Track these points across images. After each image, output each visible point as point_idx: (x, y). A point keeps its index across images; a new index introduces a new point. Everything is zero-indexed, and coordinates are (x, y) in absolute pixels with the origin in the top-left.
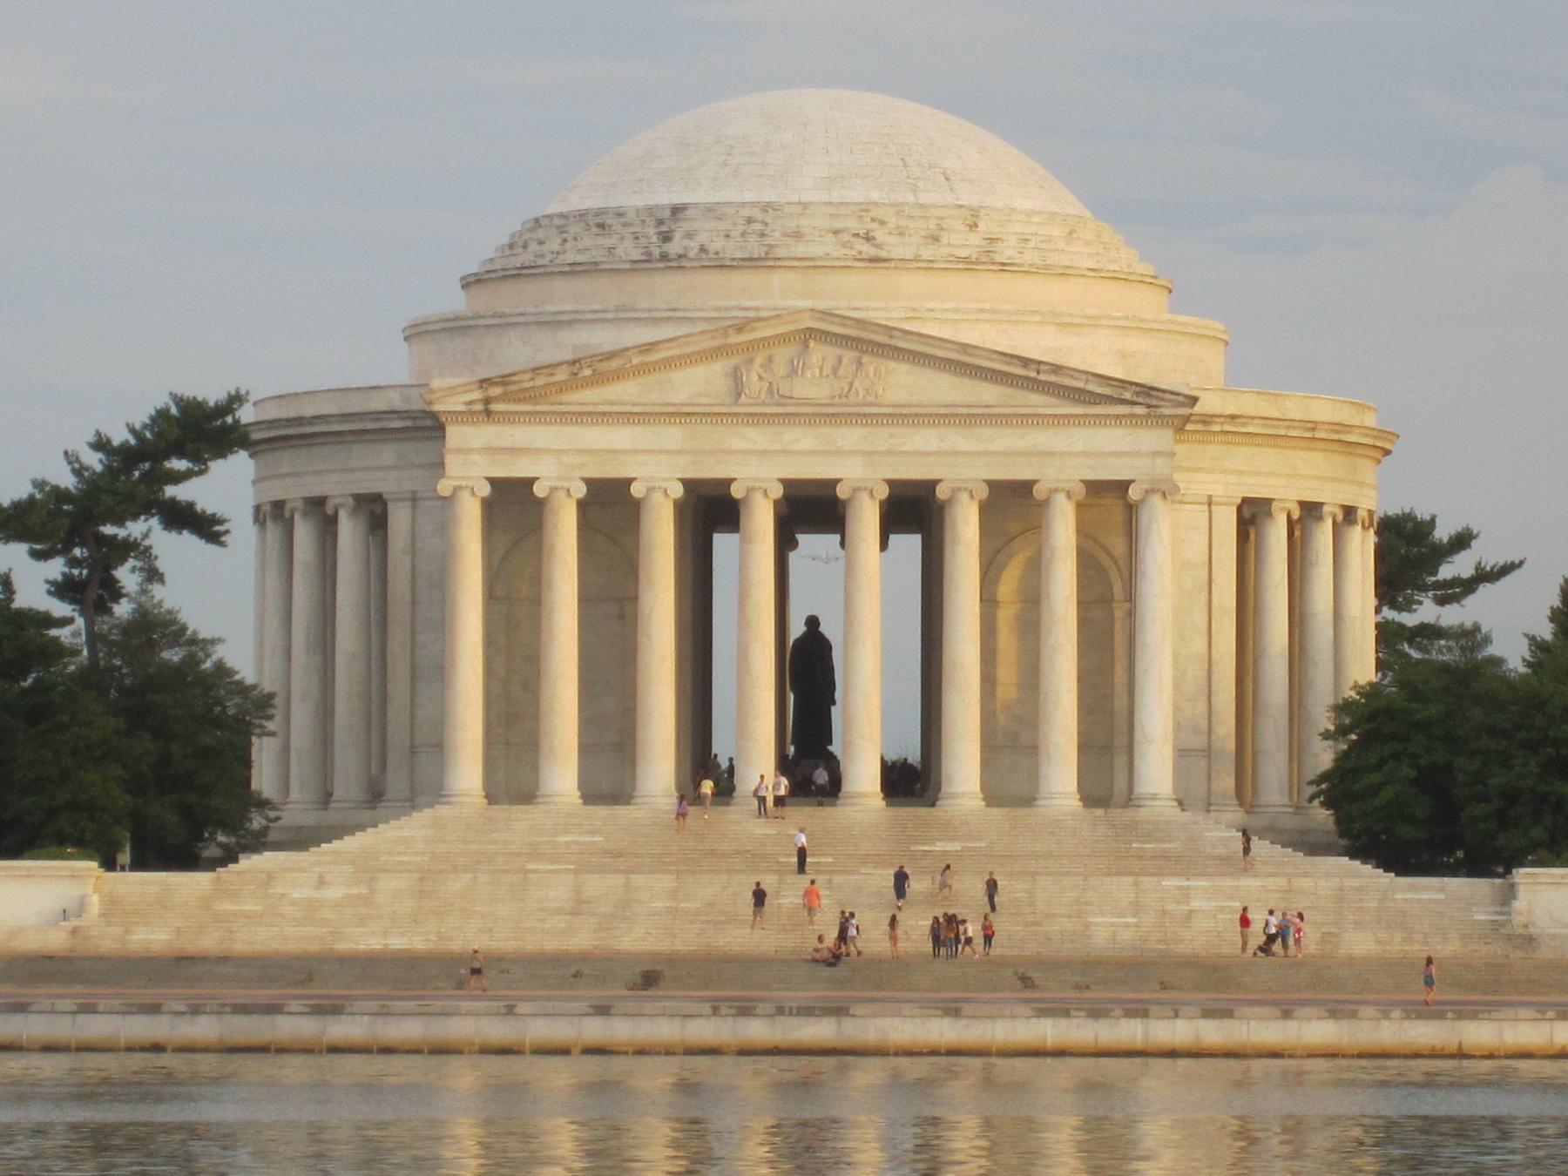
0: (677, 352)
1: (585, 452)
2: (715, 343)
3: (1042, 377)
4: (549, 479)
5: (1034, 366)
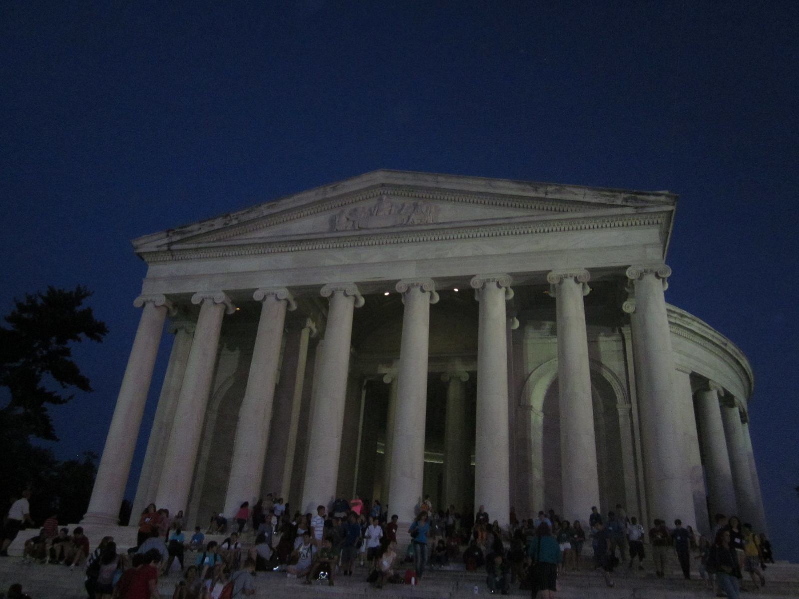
3: (550, 196)
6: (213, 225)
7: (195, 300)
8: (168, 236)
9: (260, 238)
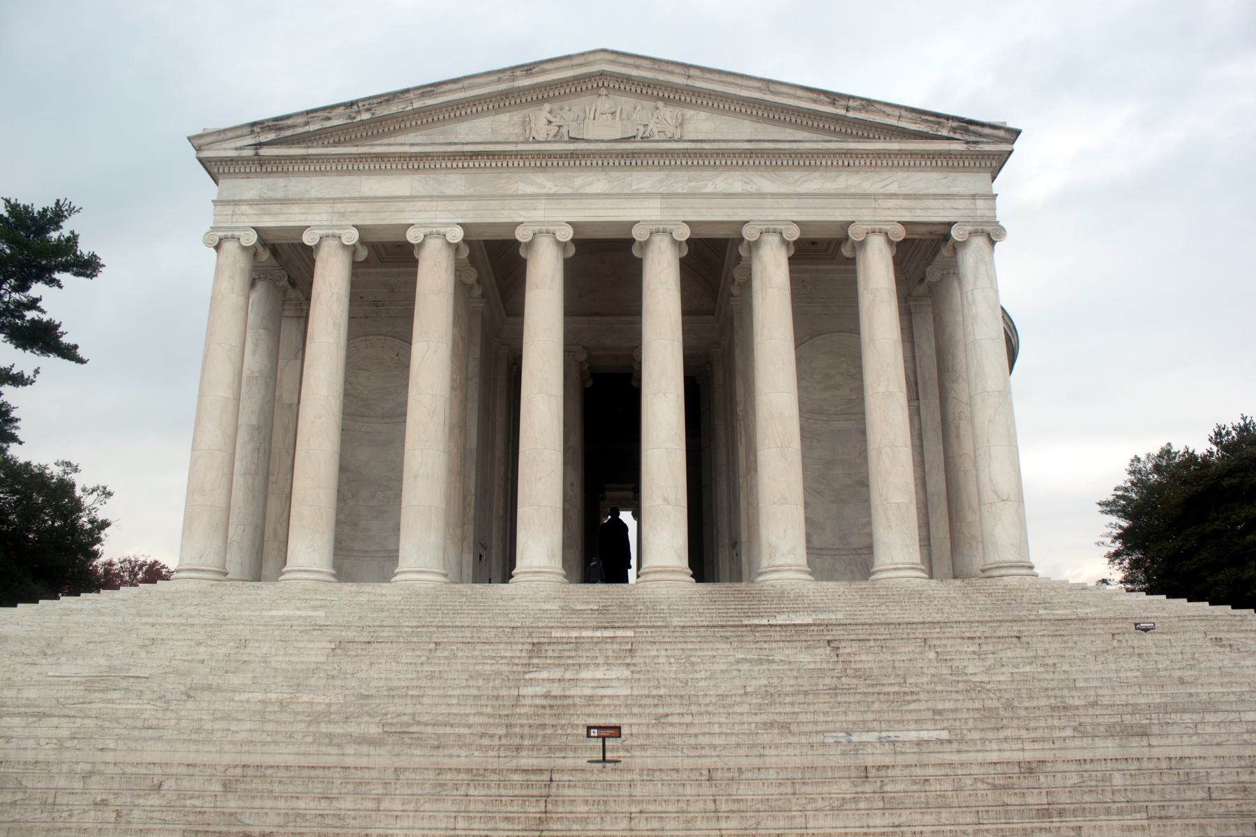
0: (461, 95)
2: (503, 86)
3: (851, 114)
4: (320, 227)
5: (843, 103)
6: (328, 119)
7: (308, 239)
8: (252, 132)
9: (412, 145)
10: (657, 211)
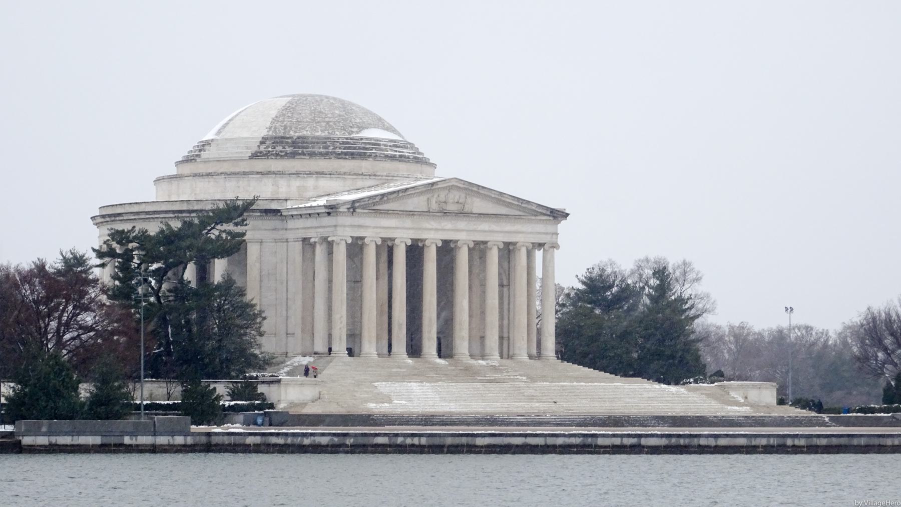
1: (380, 227)
10: (464, 233)
